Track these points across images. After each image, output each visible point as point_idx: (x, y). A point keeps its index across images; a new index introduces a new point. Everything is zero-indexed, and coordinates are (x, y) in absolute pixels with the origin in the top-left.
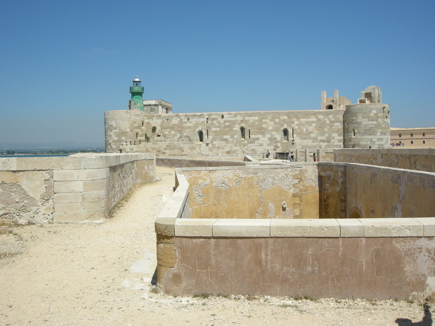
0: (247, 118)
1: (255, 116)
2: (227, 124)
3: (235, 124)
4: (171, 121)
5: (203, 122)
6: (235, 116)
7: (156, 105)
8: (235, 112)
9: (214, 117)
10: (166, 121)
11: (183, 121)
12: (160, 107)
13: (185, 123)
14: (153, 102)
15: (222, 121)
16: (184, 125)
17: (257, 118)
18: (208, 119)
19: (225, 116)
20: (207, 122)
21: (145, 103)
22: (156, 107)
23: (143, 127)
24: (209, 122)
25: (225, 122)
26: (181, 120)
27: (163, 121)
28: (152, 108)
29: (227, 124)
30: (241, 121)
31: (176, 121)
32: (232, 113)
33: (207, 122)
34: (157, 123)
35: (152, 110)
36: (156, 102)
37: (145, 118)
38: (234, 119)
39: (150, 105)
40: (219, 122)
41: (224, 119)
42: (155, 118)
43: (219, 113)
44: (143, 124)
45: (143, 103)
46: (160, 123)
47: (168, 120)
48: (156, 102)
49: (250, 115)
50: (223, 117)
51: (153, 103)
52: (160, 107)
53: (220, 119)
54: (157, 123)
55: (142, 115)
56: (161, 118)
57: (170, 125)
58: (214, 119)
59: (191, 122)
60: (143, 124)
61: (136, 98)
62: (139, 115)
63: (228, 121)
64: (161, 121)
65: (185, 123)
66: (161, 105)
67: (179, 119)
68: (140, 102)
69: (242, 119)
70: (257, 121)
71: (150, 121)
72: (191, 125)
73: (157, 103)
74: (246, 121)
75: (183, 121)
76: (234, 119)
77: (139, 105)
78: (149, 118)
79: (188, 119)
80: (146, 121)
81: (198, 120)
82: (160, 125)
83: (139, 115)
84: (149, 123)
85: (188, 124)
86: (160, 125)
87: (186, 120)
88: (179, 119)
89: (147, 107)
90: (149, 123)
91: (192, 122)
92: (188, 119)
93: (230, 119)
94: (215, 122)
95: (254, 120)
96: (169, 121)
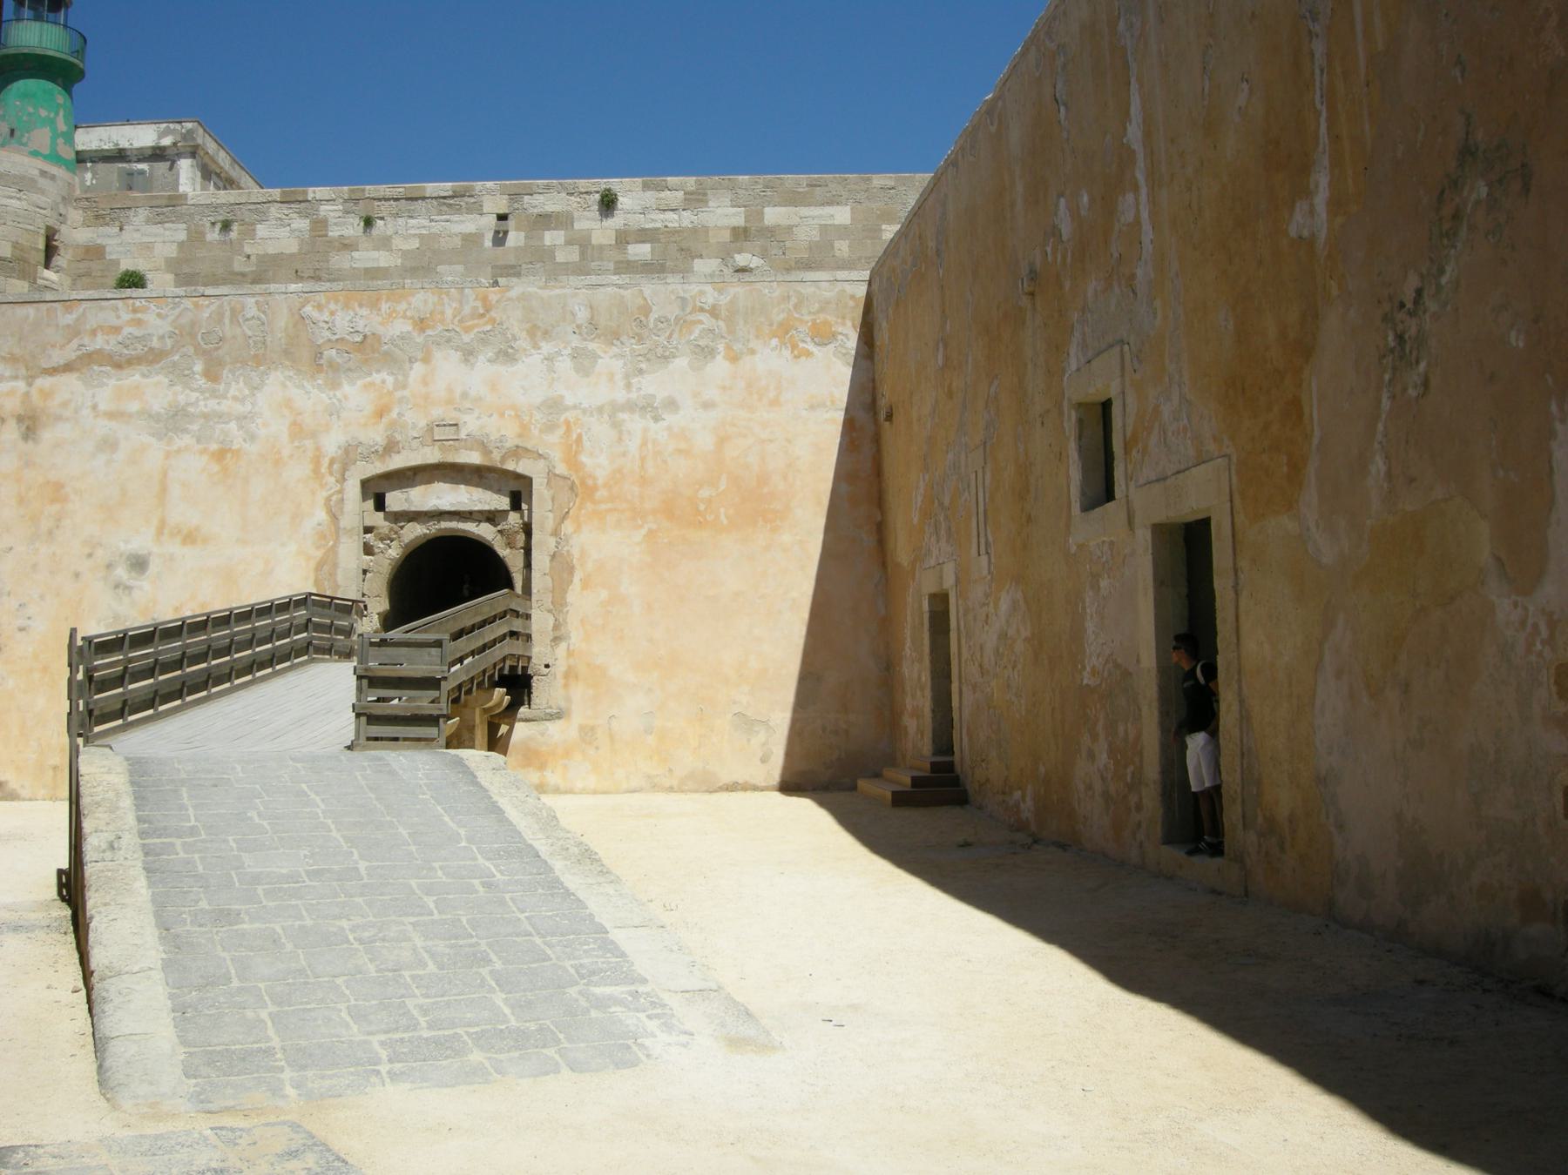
0: (773, 215)
1: (830, 203)
2: (640, 251)
3: (690, 254)
4: (250, 232)
5: (471, 240)
6: (695, 200)
7: (157, 154)
8: (691, 182)
9: (549, 208)
10: (214, 235)
11: (334, 233)
12: (185, 166)
13: (347, 246)
14: (143, 136)
15: (602, 231)
16: (340, 261)
17: (842, 215)
18: (502, 218)
19: (624, 202)
20: (500, 238)
21: (92, 139)
22: (162, 166)
23: (48, 274)
24: (515, 238)
25: (623, 238)
26: (320, 225)
27: (196, 237)
28: (131, 174)
29: (640, 251)
30: (735, 230)
31: (283, 232)
32: (672, 180)
33: (500, 238)
34: (148, 247)
35: (130, 182)
36: (162, 135)
37: (75, 215)
38: (687, 219)
39: (120, 155)
40: (583, 243)
41: (617, 221)
42: (143, 213)
43: (583, 184)
44: (50, 251)
45: (70, 140)
46: (172, 251)
47: (226, 226)
48: (162, 135)
49: (794, 199)
50: (608, 204)
51: (137, 145)
52: (185, 166)
53: (589, 222)
54: (148, 247)
55: (43, 182)
56: (179, 218)
57: (239, 264)
58: (546, 221)
59: (385, 244)
60: (50, 251)
61: (25, 96)
62: (23, 184)
63: (644, 235)
64: (182, 236)
65: (347, 246)
66: (193, 155)
67: (303, 224)
68: (52, 122)
69: (740, 221)
70: (842, 232)
71: (106, 236)
72: (383, 259)
73: (167, 141)
74: (771, 232)
75: (334, 233)
76: (687, 219)
77: (41, 138)
78: (99, 219)
79: (368, 222)
80: (76, 233)
81: (436, 228)
82: (173, 265)
83: (23, 184)
84: (95, 252)
85: (367, 257)
86: (173, 265)
87: (353, 227)
88: (303, 224)
89: (101, 166)
90: (95, 252)
91: (398, 243)
92: (368, 222)
93: (657, 220)
94: (552, 238)
95: (824, 229)
96: (233, 235)
